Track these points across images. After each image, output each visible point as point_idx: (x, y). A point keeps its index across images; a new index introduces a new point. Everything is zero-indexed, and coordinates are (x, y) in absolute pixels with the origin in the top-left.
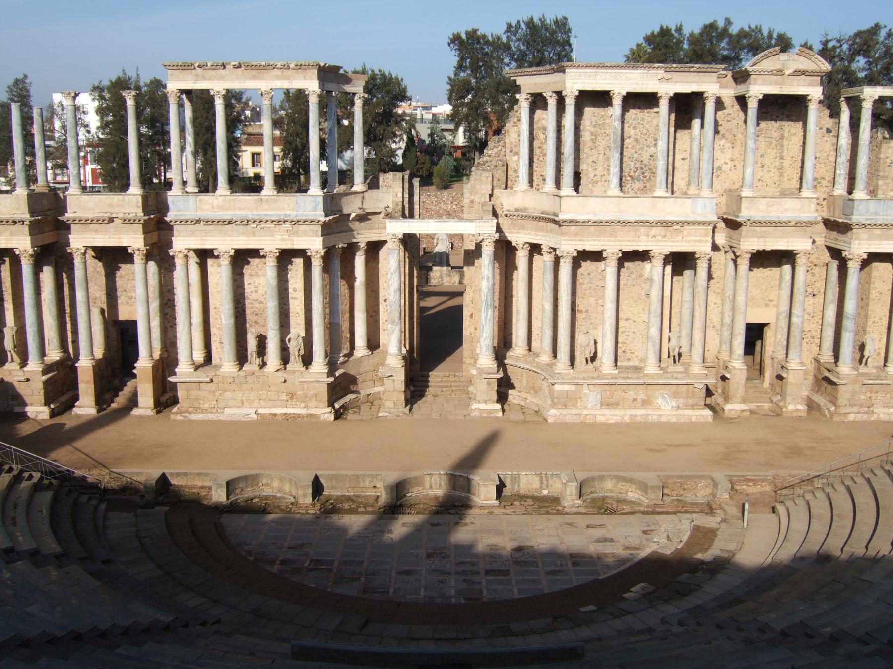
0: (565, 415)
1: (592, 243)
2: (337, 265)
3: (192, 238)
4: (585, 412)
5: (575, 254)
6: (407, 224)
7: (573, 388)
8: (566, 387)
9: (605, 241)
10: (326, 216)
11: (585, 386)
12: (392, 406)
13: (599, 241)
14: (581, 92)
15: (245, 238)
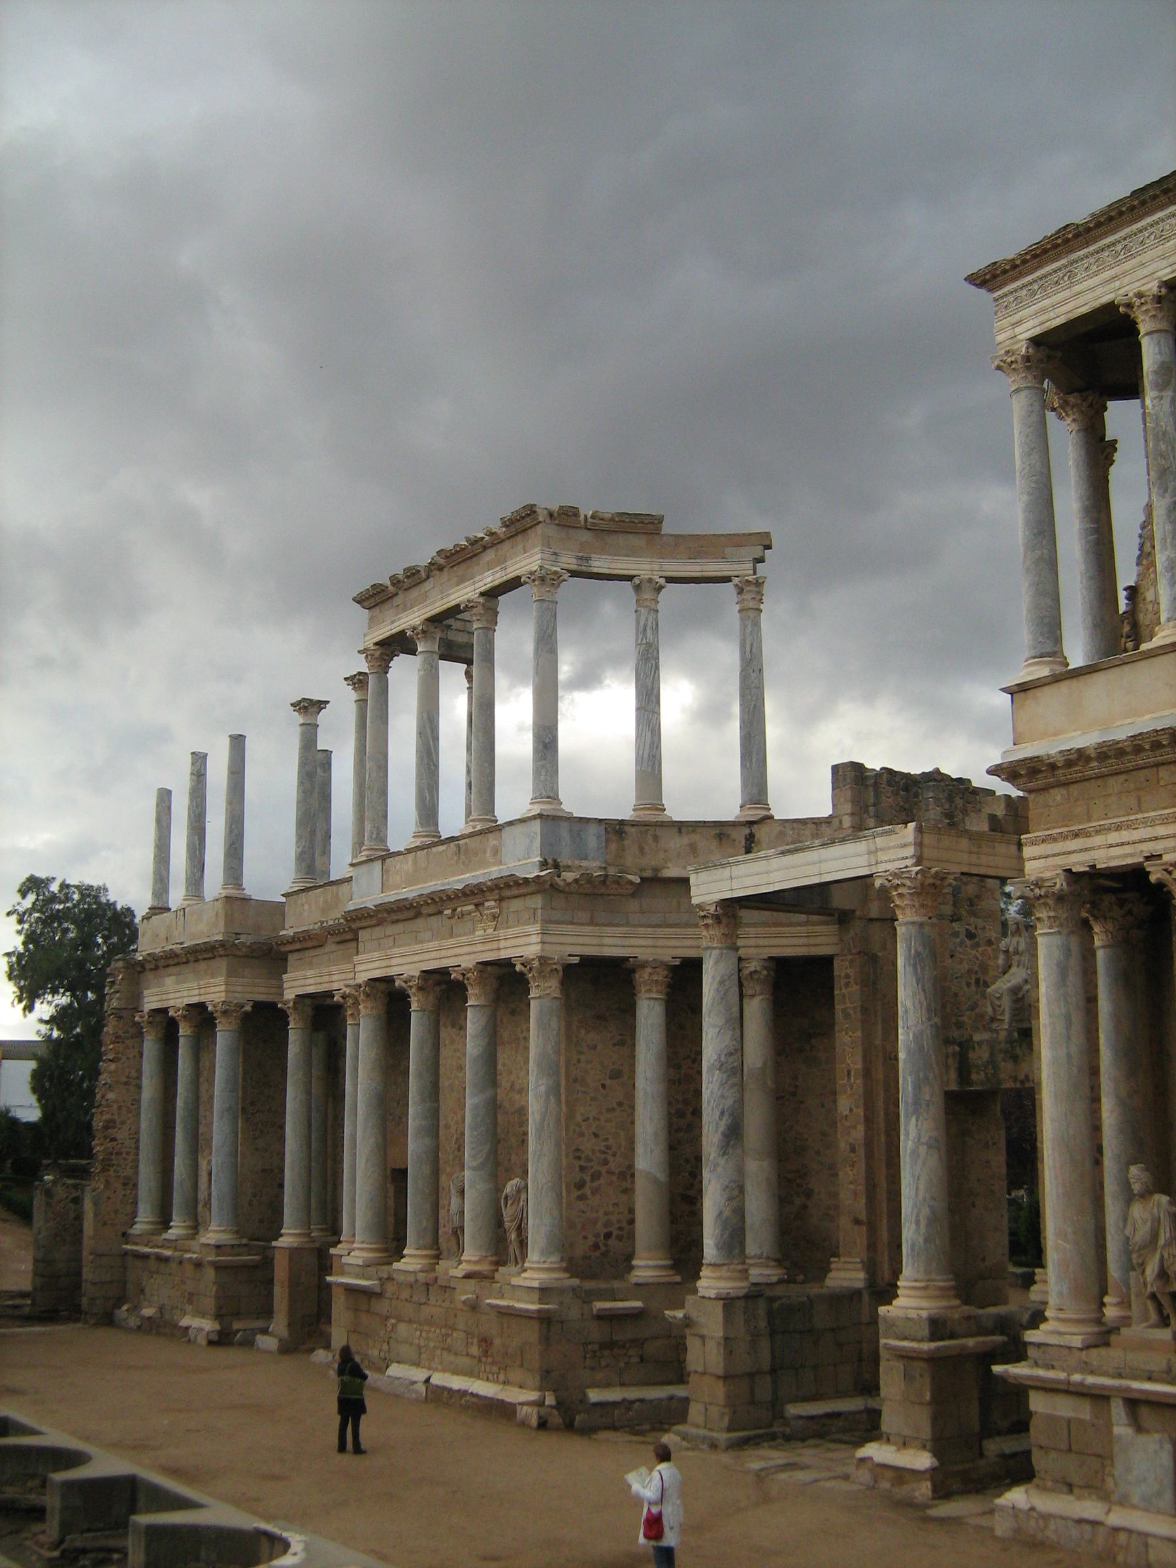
0: (1046, 1517)
1: (1114, 837)
2: (650, 1015)
3: (376, 954)
4: (1116, 1518)
5: (1060, 883)
6: (726, 872)
7: (1083, 1411)
8: (1064, 1408)
9: (1152, 823)
10: (544, 864)
11: (1117, 1409)
12: (700, 1419)
13: (1129, 826)
14: (1036, 341)
15: (433, 944)
